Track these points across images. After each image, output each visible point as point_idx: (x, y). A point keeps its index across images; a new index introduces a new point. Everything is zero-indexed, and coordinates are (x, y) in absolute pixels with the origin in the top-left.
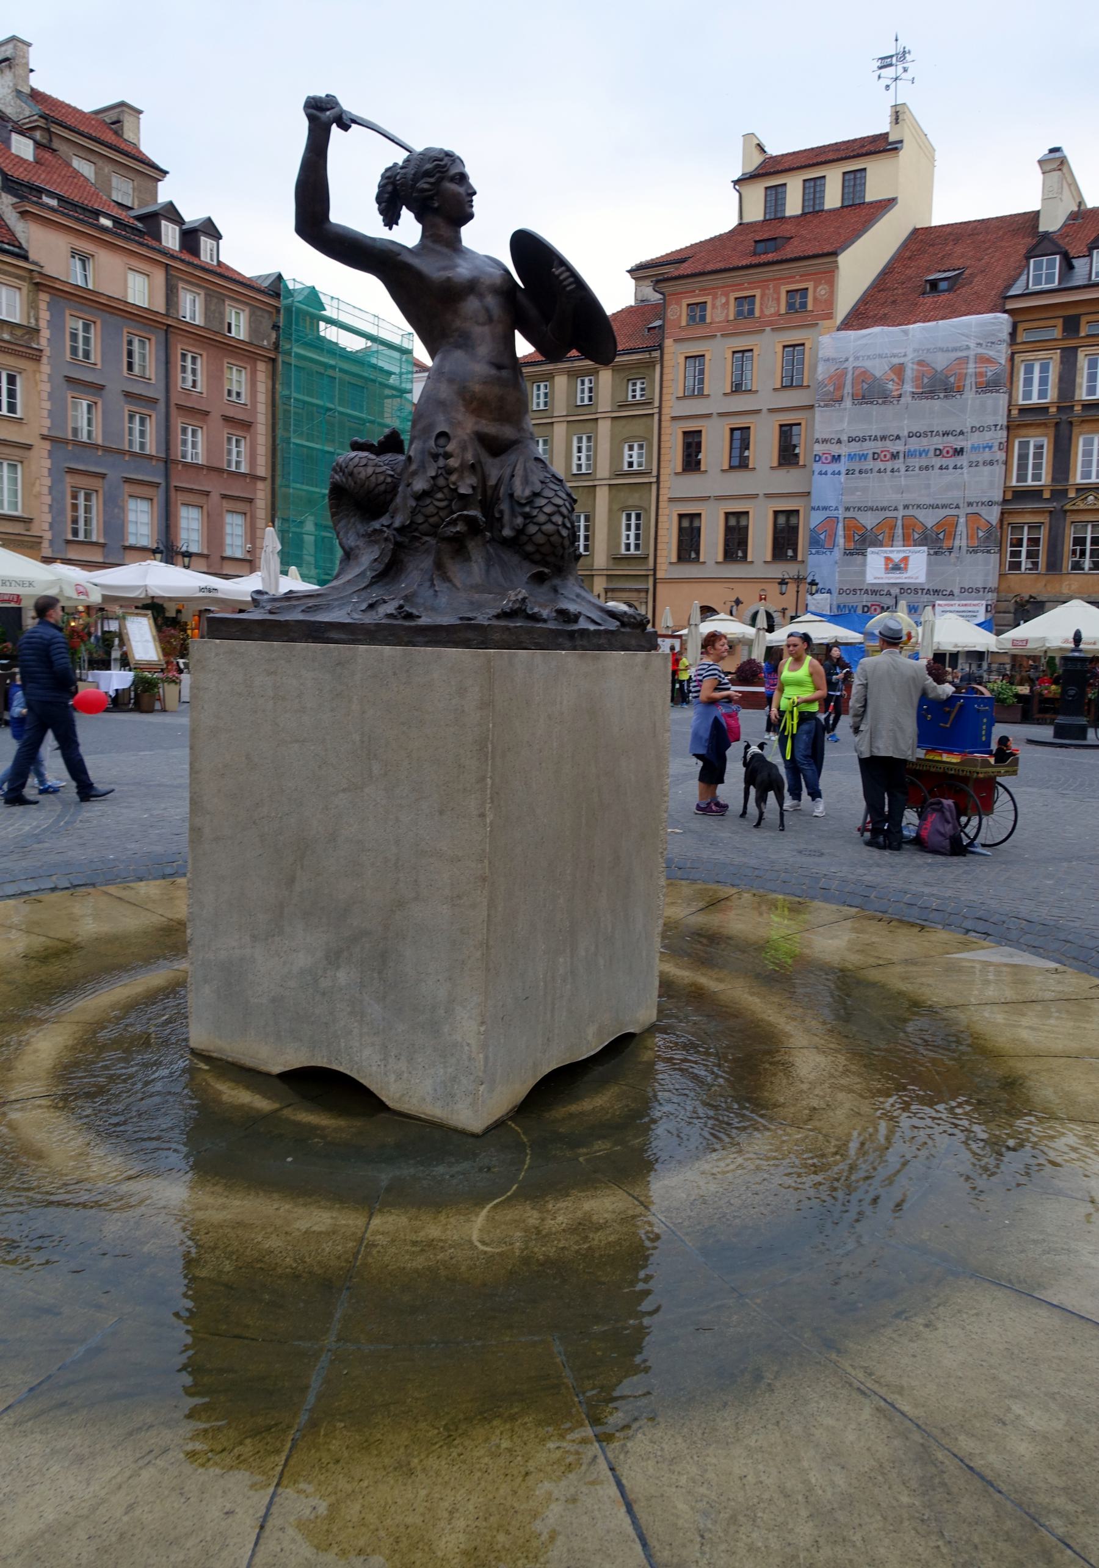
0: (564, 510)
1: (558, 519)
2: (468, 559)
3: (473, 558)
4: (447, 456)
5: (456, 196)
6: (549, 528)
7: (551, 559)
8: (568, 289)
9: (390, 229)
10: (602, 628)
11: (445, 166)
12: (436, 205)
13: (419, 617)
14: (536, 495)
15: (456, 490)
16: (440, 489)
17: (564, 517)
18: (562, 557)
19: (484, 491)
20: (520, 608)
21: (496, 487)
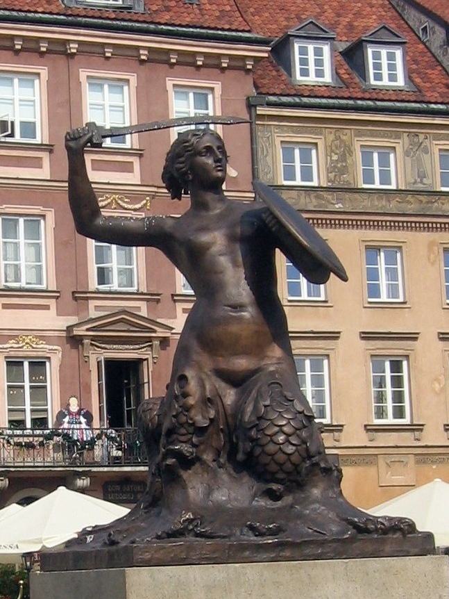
0: (285, 429)
1: (281, 438)
2: (184, 487)
3: (190, 485)
4: (185, 395)
5: (204, 168)
6: (271, 448)
7: (281, 476)
8: (274, 229)
9: (180, 199)
10: (321, 538)
11: (193, 144)
12: (191, 177)
13: (118, 543)
14: (260, 418)
15: (193, 424)
16: (182, 425)
17: (288, 435)
18: (299, 473)
19: (227, 424)
20: (186, 528)
21: (234, 416)
